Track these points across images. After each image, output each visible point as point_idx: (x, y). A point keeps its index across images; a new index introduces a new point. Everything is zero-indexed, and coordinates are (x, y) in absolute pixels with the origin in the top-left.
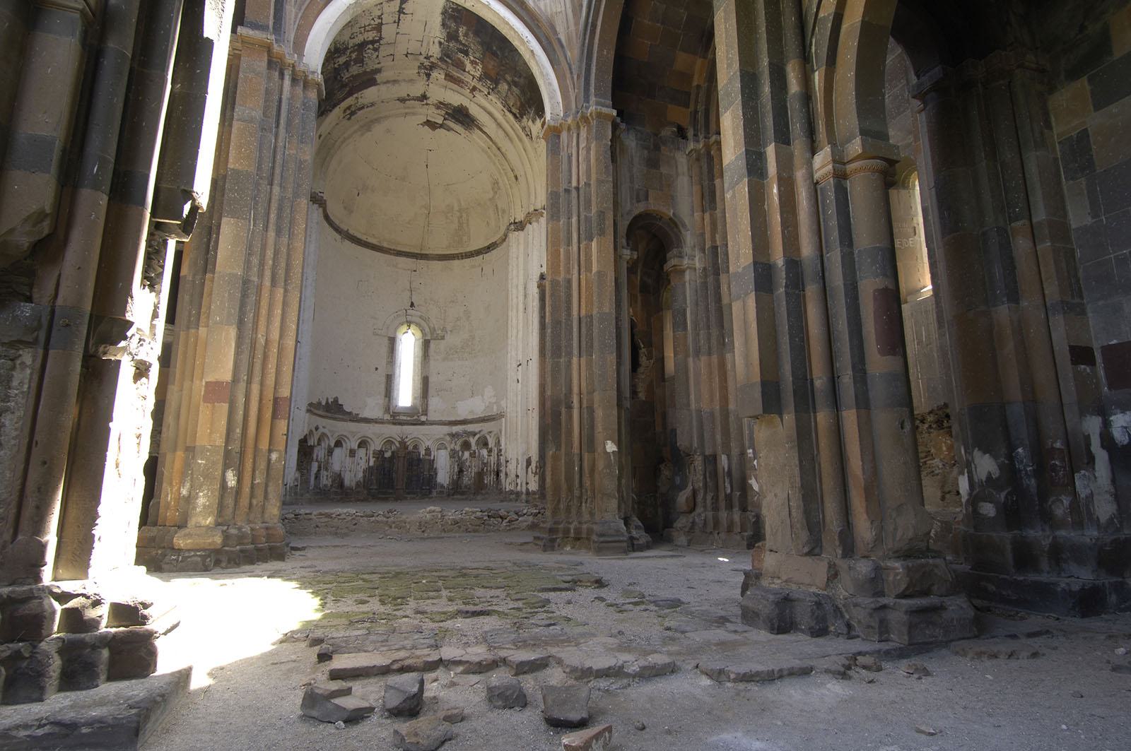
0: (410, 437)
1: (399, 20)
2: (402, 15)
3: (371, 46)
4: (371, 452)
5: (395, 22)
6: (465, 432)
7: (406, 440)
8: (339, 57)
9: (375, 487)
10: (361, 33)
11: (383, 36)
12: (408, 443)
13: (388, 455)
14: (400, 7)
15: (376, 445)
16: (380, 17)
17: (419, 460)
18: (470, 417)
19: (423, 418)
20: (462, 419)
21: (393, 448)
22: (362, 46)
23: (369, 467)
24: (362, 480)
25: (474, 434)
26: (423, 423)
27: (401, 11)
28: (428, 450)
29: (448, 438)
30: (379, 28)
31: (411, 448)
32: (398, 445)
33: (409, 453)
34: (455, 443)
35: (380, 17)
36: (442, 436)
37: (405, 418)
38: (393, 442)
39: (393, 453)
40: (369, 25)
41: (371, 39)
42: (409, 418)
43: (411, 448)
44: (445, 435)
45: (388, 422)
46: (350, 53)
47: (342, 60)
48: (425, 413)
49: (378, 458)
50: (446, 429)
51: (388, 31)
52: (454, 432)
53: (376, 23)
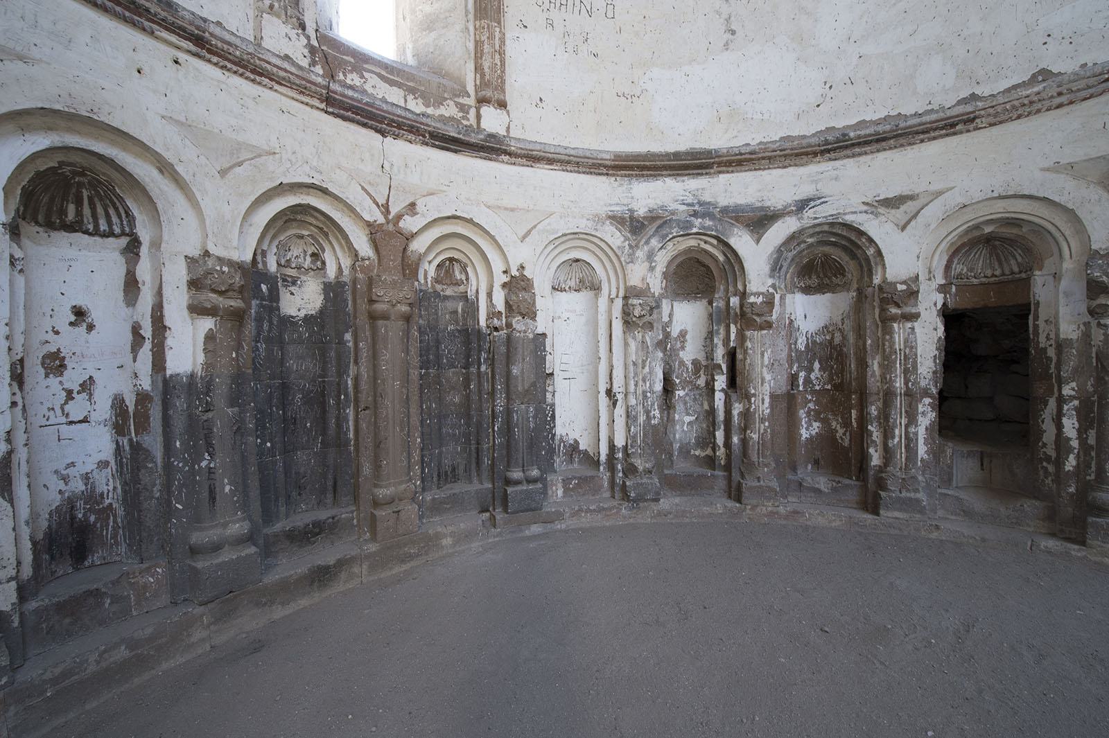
0: (429, 209)
4: (176, 277)
6: (704, 210)
7: (410, 224)
9: (238, 527)
12: (419, 245)
13: (303, 300)
15: (209, 221)
17: (470, 337)
18: (720, 140)
19: (492, 121)
20: (681, 144)
21: (335, 263)
23: (168, 386)
24: (107, 483)
25: (759, 221)
26: (491, 148)
28: (518, 285)
29: (615, 237)
31: (429, 270)
32: (363, 246)
33: (424, 299)
34: (650, 257)
36: (584, 225)
37: (394, 96)
38: (329, 227)
39: (333, 291)
42: (416, 106)
43: (429, 270)
44: (598, 219)
45: (301, 87)
48: (492, 93)
49: (238, 317)
50: (606, 194)
52: (641, 212)
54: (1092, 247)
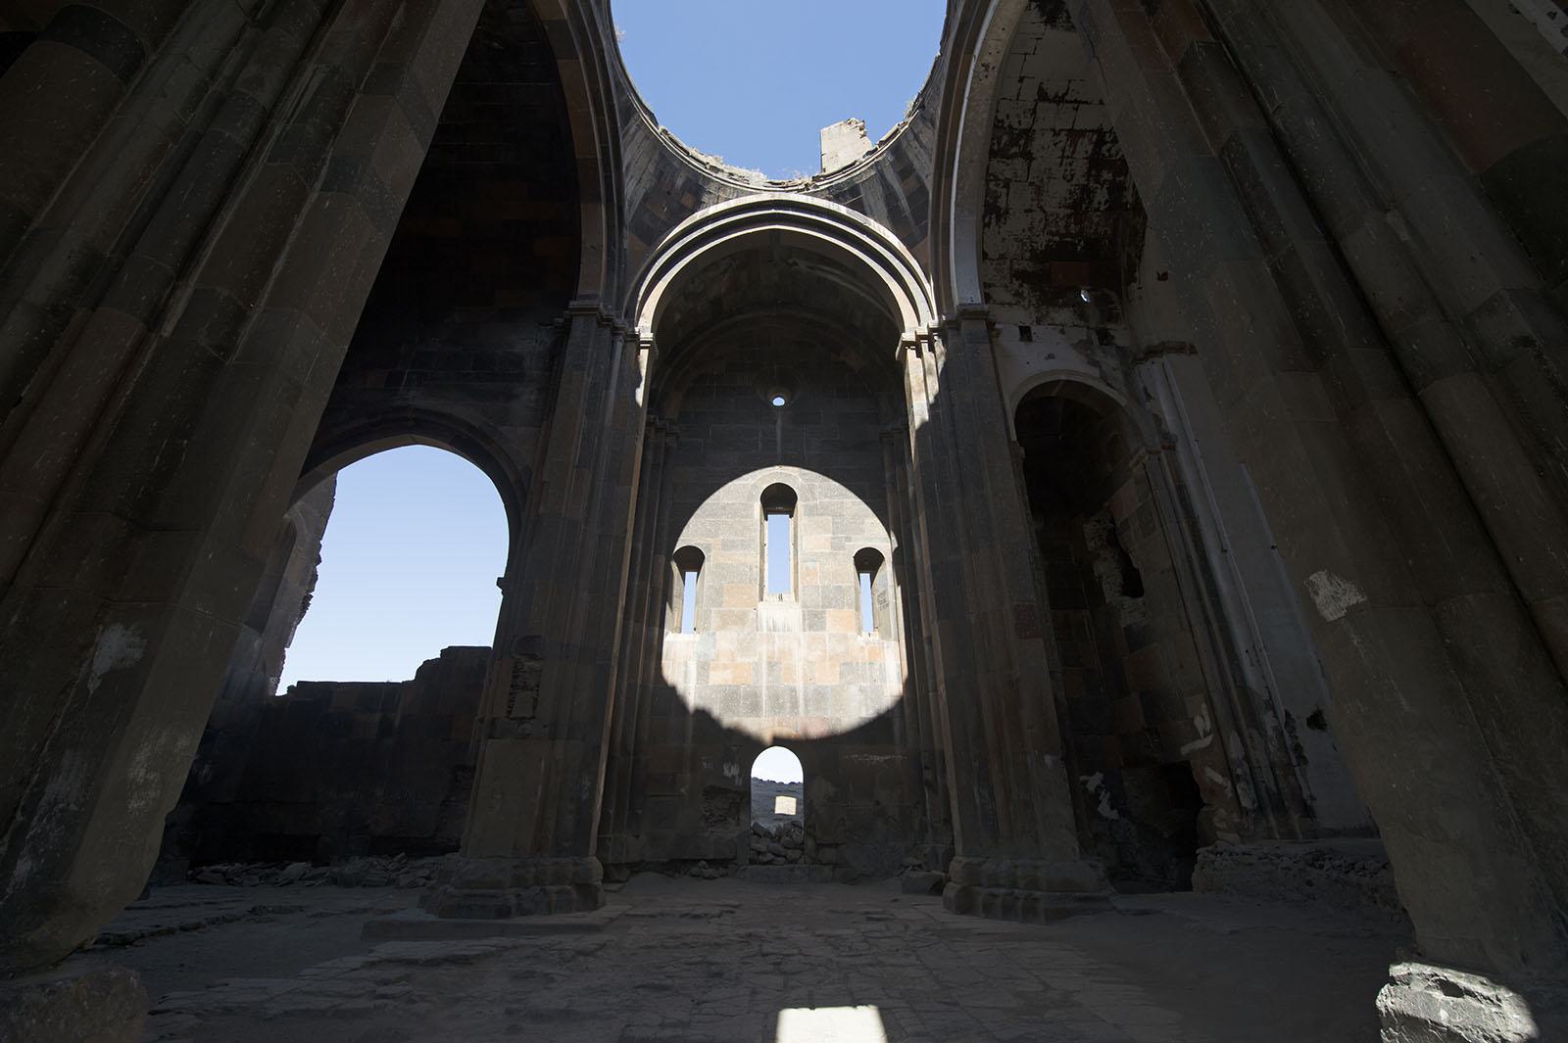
1: (1076, 101)
2: (1067, 98)
3: (1105, 148)
5: (1076, 109)
8: (1091, 201)
10: (1071, 165)
11: (1095, 128)
14: (1050, 101)
16: (1056, 133)
22: (1096, 162)
27: (1059, 100)
30: (1074, 135)
35: (1056, 133)
40: (1063, 151)
41: (1090, 148)
46: (1097, 182)
47: (1101, 196)
51: (1086, 120)
53: (1065, 138)
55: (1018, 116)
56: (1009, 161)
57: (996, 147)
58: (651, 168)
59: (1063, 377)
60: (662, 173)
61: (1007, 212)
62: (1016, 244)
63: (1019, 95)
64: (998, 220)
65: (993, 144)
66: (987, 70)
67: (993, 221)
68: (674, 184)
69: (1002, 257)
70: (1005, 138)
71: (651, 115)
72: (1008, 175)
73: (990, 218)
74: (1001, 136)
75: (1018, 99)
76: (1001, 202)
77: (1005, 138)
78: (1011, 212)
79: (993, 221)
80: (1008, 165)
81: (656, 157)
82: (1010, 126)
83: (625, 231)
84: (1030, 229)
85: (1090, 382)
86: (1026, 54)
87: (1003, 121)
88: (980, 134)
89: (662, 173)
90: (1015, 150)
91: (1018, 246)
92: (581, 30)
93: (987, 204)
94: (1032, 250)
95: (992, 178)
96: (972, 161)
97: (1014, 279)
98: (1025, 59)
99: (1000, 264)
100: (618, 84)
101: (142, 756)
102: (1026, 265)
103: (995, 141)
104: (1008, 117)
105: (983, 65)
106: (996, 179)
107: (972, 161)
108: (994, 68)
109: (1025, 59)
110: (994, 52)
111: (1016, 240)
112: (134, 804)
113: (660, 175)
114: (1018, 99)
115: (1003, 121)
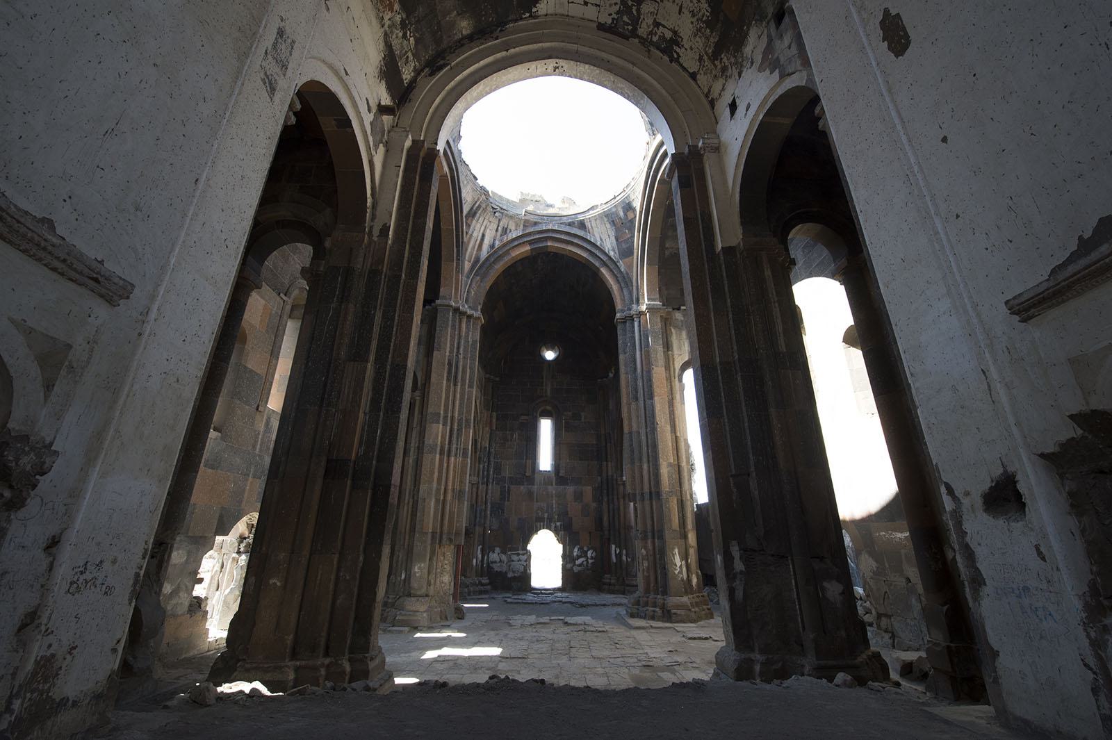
54: (8, 425)
55: (611, 5)
56: (642, 17)
57: (630, 28)
58: (608, 226)
59: (761, 117)
60: (613, 221)
61: (675, 32)
62: (698, 39)
63: (597, 5)
64: (678, 45)
65: (628, 28)
66: (558, 68)
67: (678, 50)
68: (620, 218)
69: (701, 59)
70: (625, 18)
71: (592, 208)
72: (650, 21)
73: (675, 51)
74: (624, 21)
75: (599, 6)
76: (669, 35)
77: (625, 18)
78: (676, 29)
79: (678, 50)
80: (644, 19)
81: (606, 219)
82: (617, 13)
83: (618, 264)
84: (693, 16)
85: (780, 91)
86: (569, 3)
87: (613, 19)
88: (598, 71)
89: (613, 221)
90: (635, 13)
91: (700, 37)
92: (540, 240)
93: (663, 51)
94: (708, 23)
95: (650, 37)
96: (614, 82)
97: (716, 62)
98: (573, 2)
99: (704, 66)
100: (570, 224)
101: (416, 568)
102: (714, 40)
103: (626, 27)
104: (610, 15)
105: (555, 71)
106: (651, 33)
107: (614, 82)
108: (557, 63)
109: (573, 2)
110: (546, 66)
111: (695, 36)
112: (417, 575)
113: (613, 223)
114: (599, 6)
115: (613, 19)
